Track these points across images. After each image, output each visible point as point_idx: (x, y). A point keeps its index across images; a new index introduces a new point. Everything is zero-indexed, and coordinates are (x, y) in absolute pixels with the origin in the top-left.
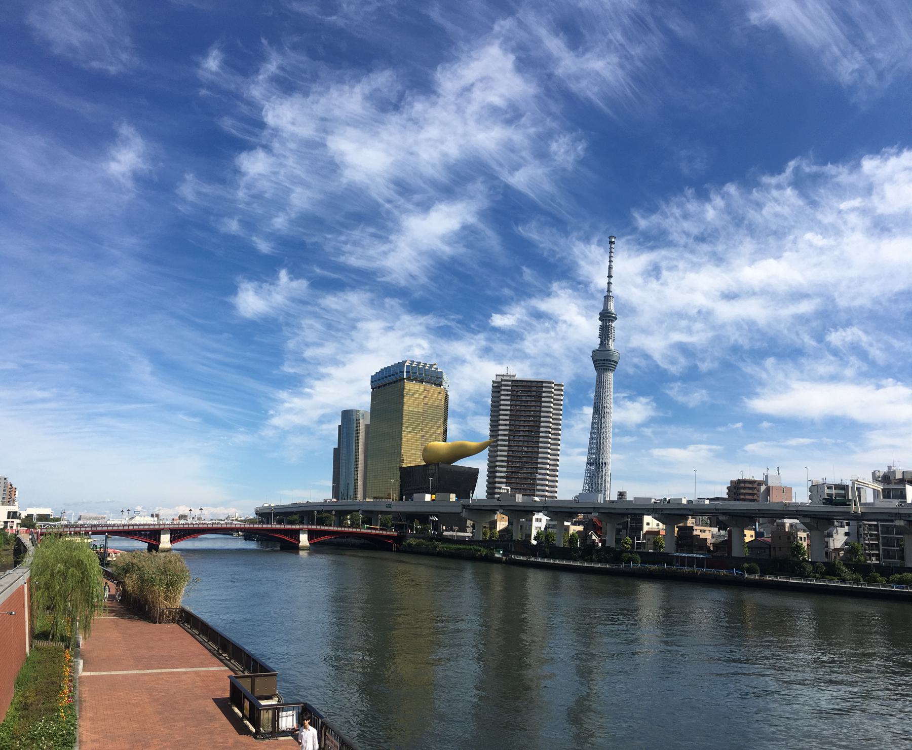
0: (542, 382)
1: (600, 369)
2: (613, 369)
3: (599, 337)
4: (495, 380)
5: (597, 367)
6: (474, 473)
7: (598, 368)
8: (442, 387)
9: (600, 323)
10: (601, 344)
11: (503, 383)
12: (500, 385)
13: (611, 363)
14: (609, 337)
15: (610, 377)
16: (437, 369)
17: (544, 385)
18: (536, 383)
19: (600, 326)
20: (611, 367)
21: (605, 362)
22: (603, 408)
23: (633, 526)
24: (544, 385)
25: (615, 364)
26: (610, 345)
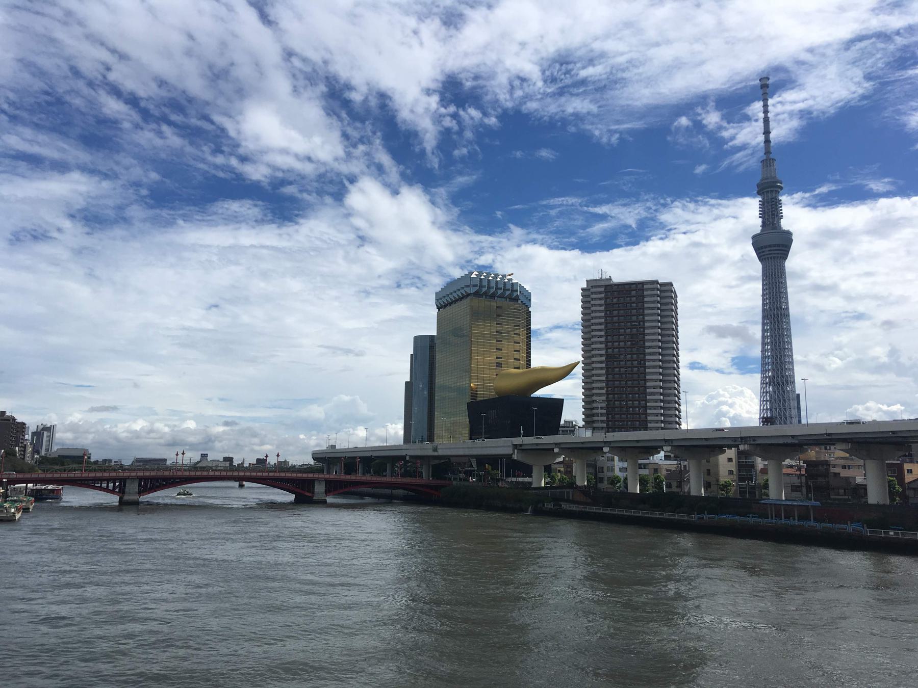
3: (760, 217)
4: (585, 286)
5: (761, 256)
6: (557, 405)
7: (763, 257)
8: (519, 302)
10: (764, 225)
14: (773, 215)
17: (645, 287)
21: (764, 250)
23: (743, 462)
25: (786, 249)
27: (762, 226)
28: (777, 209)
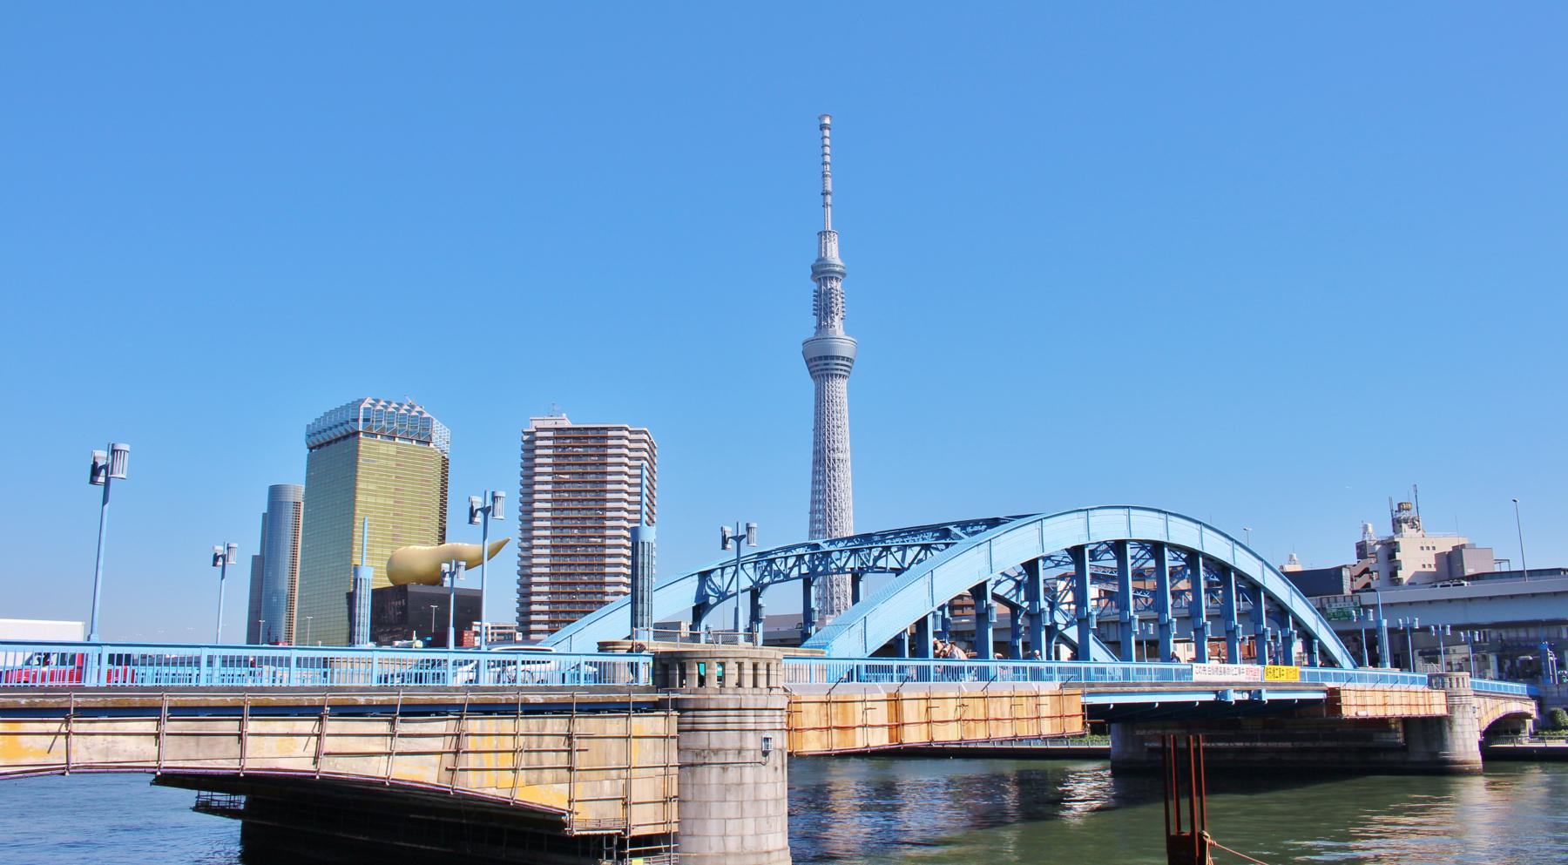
0: (606, 429)
1: (819, 376)
2: (845, 373)
3: (814, 314)
7: (814, 374)
8: (431, 445)
9: (815, 286)
11: (539, 434)
12: (533, 438)
13: (845, 363)
15: (840, 388)
16: (421, 413)
17: (610, 433)
18: (595, 431)
19: (815, 291)
20: (841, 370)
22: (832, 452)
24: (610, 433)
26: (837, 327)
27: (816, 328)
28: (837, 305)
